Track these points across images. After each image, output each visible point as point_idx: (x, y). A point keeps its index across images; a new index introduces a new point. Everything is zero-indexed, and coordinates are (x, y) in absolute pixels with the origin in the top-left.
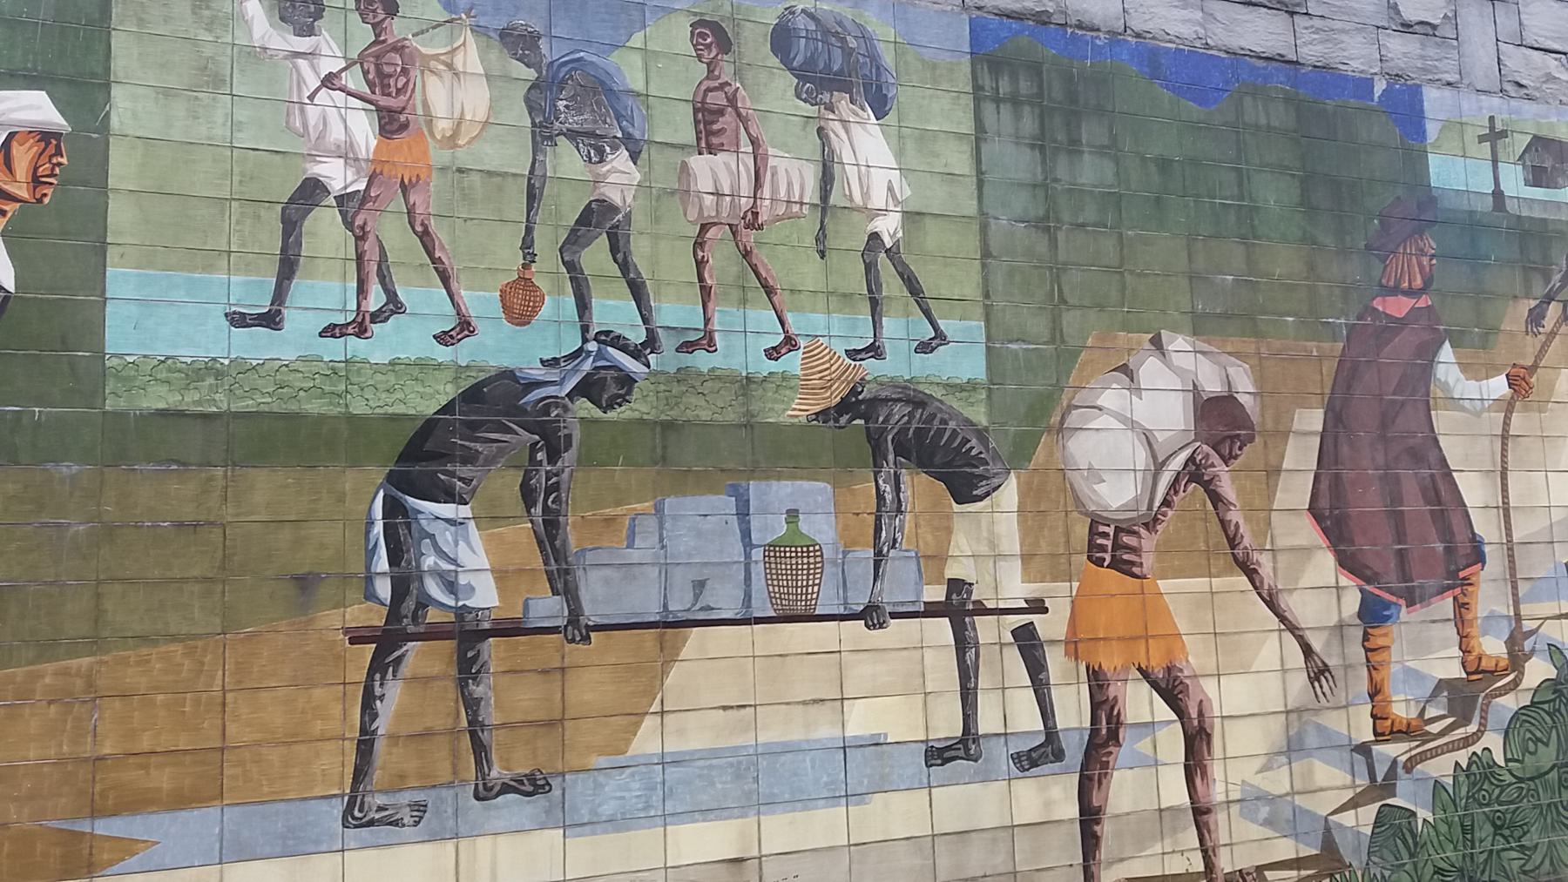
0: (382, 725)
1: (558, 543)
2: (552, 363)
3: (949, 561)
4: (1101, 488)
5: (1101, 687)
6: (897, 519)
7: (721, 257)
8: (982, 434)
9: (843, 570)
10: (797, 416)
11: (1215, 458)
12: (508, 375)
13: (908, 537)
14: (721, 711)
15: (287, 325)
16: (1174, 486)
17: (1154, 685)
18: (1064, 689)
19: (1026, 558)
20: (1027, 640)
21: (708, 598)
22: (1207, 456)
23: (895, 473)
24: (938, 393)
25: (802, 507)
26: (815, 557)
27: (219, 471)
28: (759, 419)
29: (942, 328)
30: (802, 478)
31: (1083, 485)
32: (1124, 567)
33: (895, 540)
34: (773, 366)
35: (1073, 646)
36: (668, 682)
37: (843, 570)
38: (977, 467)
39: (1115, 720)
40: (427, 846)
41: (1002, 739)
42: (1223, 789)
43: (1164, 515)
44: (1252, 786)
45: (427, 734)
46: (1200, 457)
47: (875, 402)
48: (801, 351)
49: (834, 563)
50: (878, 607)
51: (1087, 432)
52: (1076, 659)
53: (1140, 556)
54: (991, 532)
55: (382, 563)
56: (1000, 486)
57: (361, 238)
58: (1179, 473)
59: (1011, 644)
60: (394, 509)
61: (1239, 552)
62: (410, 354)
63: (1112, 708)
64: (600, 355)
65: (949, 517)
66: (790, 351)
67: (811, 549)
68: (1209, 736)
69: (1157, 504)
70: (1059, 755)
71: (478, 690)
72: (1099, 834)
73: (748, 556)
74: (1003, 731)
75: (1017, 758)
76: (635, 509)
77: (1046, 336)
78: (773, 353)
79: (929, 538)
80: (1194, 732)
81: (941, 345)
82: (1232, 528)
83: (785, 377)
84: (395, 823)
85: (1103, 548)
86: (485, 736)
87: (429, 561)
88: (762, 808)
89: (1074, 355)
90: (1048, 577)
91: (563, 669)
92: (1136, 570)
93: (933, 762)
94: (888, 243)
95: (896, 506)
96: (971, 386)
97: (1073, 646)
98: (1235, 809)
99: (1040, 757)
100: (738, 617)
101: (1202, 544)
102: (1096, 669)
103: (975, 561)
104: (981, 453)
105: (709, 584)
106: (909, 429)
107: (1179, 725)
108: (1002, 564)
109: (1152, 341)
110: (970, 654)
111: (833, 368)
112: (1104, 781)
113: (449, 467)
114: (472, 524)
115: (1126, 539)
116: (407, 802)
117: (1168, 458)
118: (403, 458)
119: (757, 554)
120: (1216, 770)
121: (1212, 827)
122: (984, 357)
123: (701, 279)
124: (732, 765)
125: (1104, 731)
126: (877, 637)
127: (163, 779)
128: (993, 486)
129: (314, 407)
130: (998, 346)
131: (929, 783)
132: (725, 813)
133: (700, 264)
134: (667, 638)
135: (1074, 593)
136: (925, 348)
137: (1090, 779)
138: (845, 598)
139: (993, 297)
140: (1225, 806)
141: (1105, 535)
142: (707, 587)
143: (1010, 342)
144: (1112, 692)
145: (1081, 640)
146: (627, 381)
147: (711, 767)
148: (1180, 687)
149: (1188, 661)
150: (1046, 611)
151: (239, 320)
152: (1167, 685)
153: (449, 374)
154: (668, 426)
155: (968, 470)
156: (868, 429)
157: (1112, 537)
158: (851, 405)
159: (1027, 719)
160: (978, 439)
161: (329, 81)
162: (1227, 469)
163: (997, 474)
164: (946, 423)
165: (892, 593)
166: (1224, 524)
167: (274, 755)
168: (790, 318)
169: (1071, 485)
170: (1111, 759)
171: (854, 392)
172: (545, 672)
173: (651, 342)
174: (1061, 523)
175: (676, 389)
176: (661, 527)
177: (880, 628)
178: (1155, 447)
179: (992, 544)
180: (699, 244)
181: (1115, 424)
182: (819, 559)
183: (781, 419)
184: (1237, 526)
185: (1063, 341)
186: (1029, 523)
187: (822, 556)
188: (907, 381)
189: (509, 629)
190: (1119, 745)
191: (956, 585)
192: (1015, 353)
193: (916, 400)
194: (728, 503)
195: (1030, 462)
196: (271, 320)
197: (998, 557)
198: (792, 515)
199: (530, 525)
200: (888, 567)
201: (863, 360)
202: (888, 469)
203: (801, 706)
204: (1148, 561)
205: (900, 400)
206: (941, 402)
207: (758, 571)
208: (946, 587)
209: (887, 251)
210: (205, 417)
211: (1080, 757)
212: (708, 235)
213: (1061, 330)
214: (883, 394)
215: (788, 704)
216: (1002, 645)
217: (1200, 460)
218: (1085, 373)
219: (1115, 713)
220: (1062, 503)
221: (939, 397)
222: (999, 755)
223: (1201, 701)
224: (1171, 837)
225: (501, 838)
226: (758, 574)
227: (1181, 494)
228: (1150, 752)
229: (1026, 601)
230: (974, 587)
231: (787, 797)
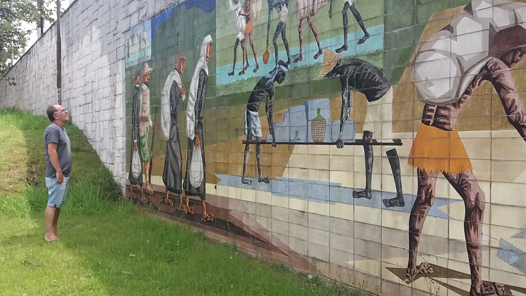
0: (246, 162)
1: (271, 121)
2: (270, 73)
3: (365, 124)
4: (432, 89)
5: (424, 179)
6: (348, 109)
7: (305, 29)
8: (380, 72)
9: (331, 128)
10: (321, 77)
11: (501, 64)
12: (264, 78)
13: (351, 116)
14: (300, 169)
15: (235, 74)
16: (472, 83)
17: (451, 182)
18: (407, 178)
19: (394, 122)
20: (392, 156)
21: (298, 137)
22: (496, 64)
23: (349, 92)
24: (364, 58)
25: (321, 107)
26: (324, 124)
27: (228, 107)
28: (311, 80)
29: (368, 31)
30: (321, 98)
31: (422, 88)
32: (440, 125)
33: (347, 117)
34: (316, 61)
35: (412, 160)
36: (290, 159)
37: (331, 128)
38: (378, 86)
39: (429, 194)
40: (252, 190)
41: (380, 193)
42: (488, 239)
43: (465, 98)
44: (506, 242)
45: (252, 165)
46: (491, 65)
47: (344, 66)
48: (323, 54)
49: (329, 125)
50: (341, 141)
51: (426, 63)
52: (413, 165)
53: (449, 120)
54: (381, 112)
55: (246, 127)
56: (386, 93)
57: (243, 50)
58: (476, 76)
59: (386, 157)
60: (248, 114)
61: (513, 116)
62: (249, 77)
63: (428, 189)
64: (279, 68)
65: (366, 107)
66: (320, 54)
67: (323, 120)
68: (481, 212)
69: (461, 93)
70: (402, 204)
71: (259, 156)
72: (417, 240)
73: (307, 124)
74: (380, 190)
75: (385, 201)
76: (284, 111)
77: (410, 22)
78: (316, 57)
79: (358, 115)
80: (472, 208)
81: (367, 38)
82: (510, 102)
83: (319, 64)
84: (248, 184)
85: (430, 117)
86: (260, 167)
87: (252, 125)
88: (309, 199)
89: (422, 27)
90: (403, 130)
91: (272, 153)
92: (446, 126)
93: (355, 196)
94: (351, 4)
95: (348, 104)
96: (377, 53)
97: (412, 160)
98: (494, 252)
99: (394, 203)
100: (305, 142)
101: (487, 113)
102: (422, 171)
103: (374, 124)
104: (379, 80)
105: (299, 132)
106: (354, 75)
107: (463, 203)
108: (384, 125)
109: (465, 9)
110: (370, 160)
111: (332, 57)
112: (422, 219)
113: (255, 103)
114: (258, 116)
115: (442, 112)
116: (249, 179)
117: (470, 69)
118: (250, 101)
119: (310, 123)
120: (484, 229)
121: (478, 256)
122: (383, 39)
123: (300, 38)
124: (302, 185)
125: (424, 198)
126: (340, 151)
128: (383, 93)
129: (238, 92)
130: (388, 33)
131: (354, 203)
132: (301, 198)
133: (300, 33)
134: (290, 147)
135: (414, 138)
136: (361, 41)
137: (415, 217)
138: (332, 137)
139: (388, 12)
140: (488, 248)
141: (432, 111)
142: (299, 133)
143: (394, 29)
144: (429, 182)
145: (416, 158)
146: (284, 74)
147: (298, 184)
148: (466, 185)
149: (472, 172)
150: (401, 144)
151: (230, 74)
152: (458, 183)
153: (255, 80)
154: (292, 86)
155: (374, 88)
156: (341, 77)
157: (435, 111)
158: (338, 69)
159: (390, 187)
160: (378, 74)
161: (240, 14)
162: (509, 69)
163: (385, 88)
164: (366, 70)
165: (345, 137)
166: (504, 101)
167: (234, 166)
168: (320, 43)
169: (417, 89)
170: (426, 211)
171: (337, 65)
172: (269, 154)
173: (289, 62)
174: (411, 106)
175: (294, 74)
176: (290, 116)
177: (341, 148)
178: (463, 64)
179: (381, 117)
180: (300, 27)
181: (441, 56)
182: (325, 124)
183: (317, 79)
184: (513, 101)
185: (417, 22)
186: (397, 107)
187: (326, 123)
188: (355, 56)
189: (264, 142)
190: (430, 205)
191: (367, 133)
192: (396, 34)
193: (357, 63)
194: (303, 107)
195: (399, 81)
196: (233, 74)
197: (383, 122)
198: (319, 110)
199: (267, 116)
200: (345, 127)
201: (341, 52)
202: (347, 91)
203: (318, 171)
204: (453, 122)
205: (352, 64)
206: (366, 62)
207: (310, 128)
208: (363, 134)
209: (350, 7)
210: (226, 96)
211: (411, 207)
212: (302, 23)
213: (417, 18)
214: (346, 63)
215: (315, 169)
216: (382, 157)
217: (491, 67)
218: (427, 35)
219: (430, 191)
220: (412, 96)
221: (365, 60)
222: (379, 199)
223: (478, 193)
224: (454, 253)
225: (262, 192)
226: (310, 129)
227: (477, 87)
228: (446, 212)
229: (393, 140)
230: (373, 133)
231: (314, 197)
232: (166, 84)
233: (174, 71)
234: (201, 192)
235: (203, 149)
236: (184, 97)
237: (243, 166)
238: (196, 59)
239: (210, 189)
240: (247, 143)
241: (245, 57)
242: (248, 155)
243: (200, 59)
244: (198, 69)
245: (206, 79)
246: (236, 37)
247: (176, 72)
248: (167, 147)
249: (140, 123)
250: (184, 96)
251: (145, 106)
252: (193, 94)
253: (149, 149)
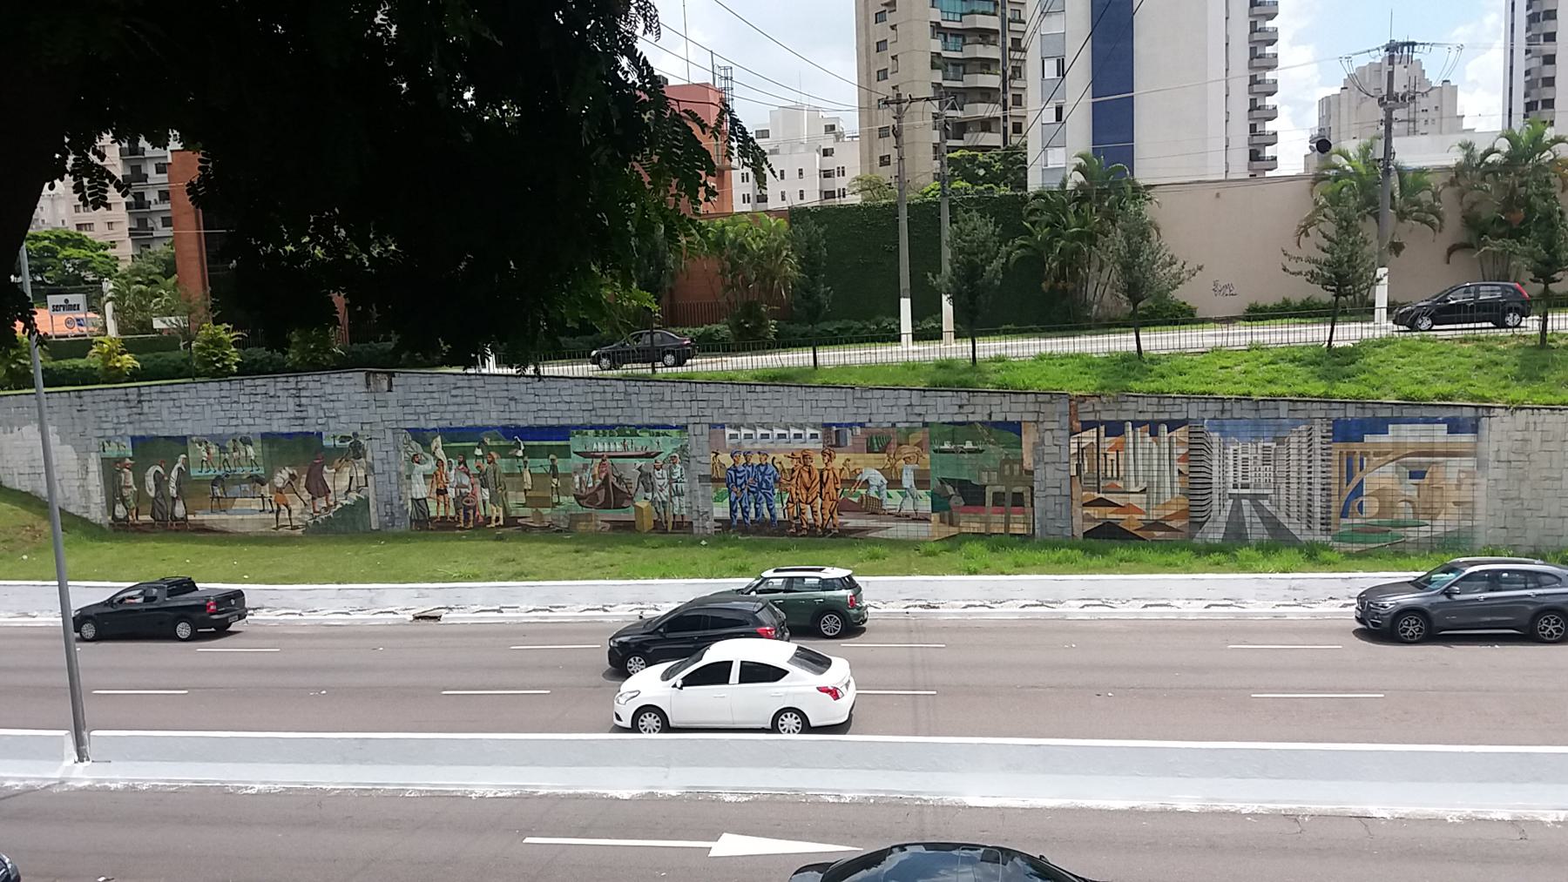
20: (270, 501)
159: (270, 508)
234: (185, 519)
238: (177, 462)
239: (190, 517)
241: (208, 467)
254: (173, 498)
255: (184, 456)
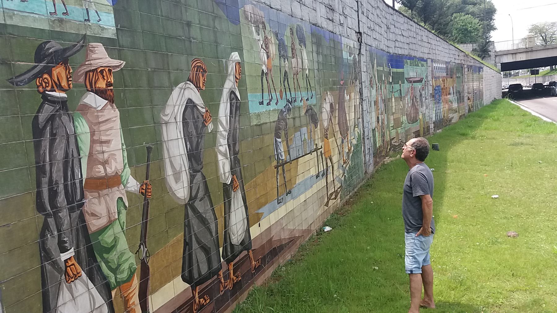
15: (264, 104)
55: (276, 153)
57: (268, 83)
87: (279, 150)
127: (263, 200)
232: (170, 102)
233: (186, 83)
235: (243, 190)
236: (210, 127)
237: (277, 188)
240: (277, 167)
242: (279, 177)
243: (228, 78)
244: (228, 90)
245: (238, 104)
246: (262, 68)
247: (192, 86)
248: (187, 216)
249: (83, 196)
250: (210, 125)
251: (105, 148)
252: (224, 123)
253: (131, 248)
254: (225, 184)
255: (235, 56)
